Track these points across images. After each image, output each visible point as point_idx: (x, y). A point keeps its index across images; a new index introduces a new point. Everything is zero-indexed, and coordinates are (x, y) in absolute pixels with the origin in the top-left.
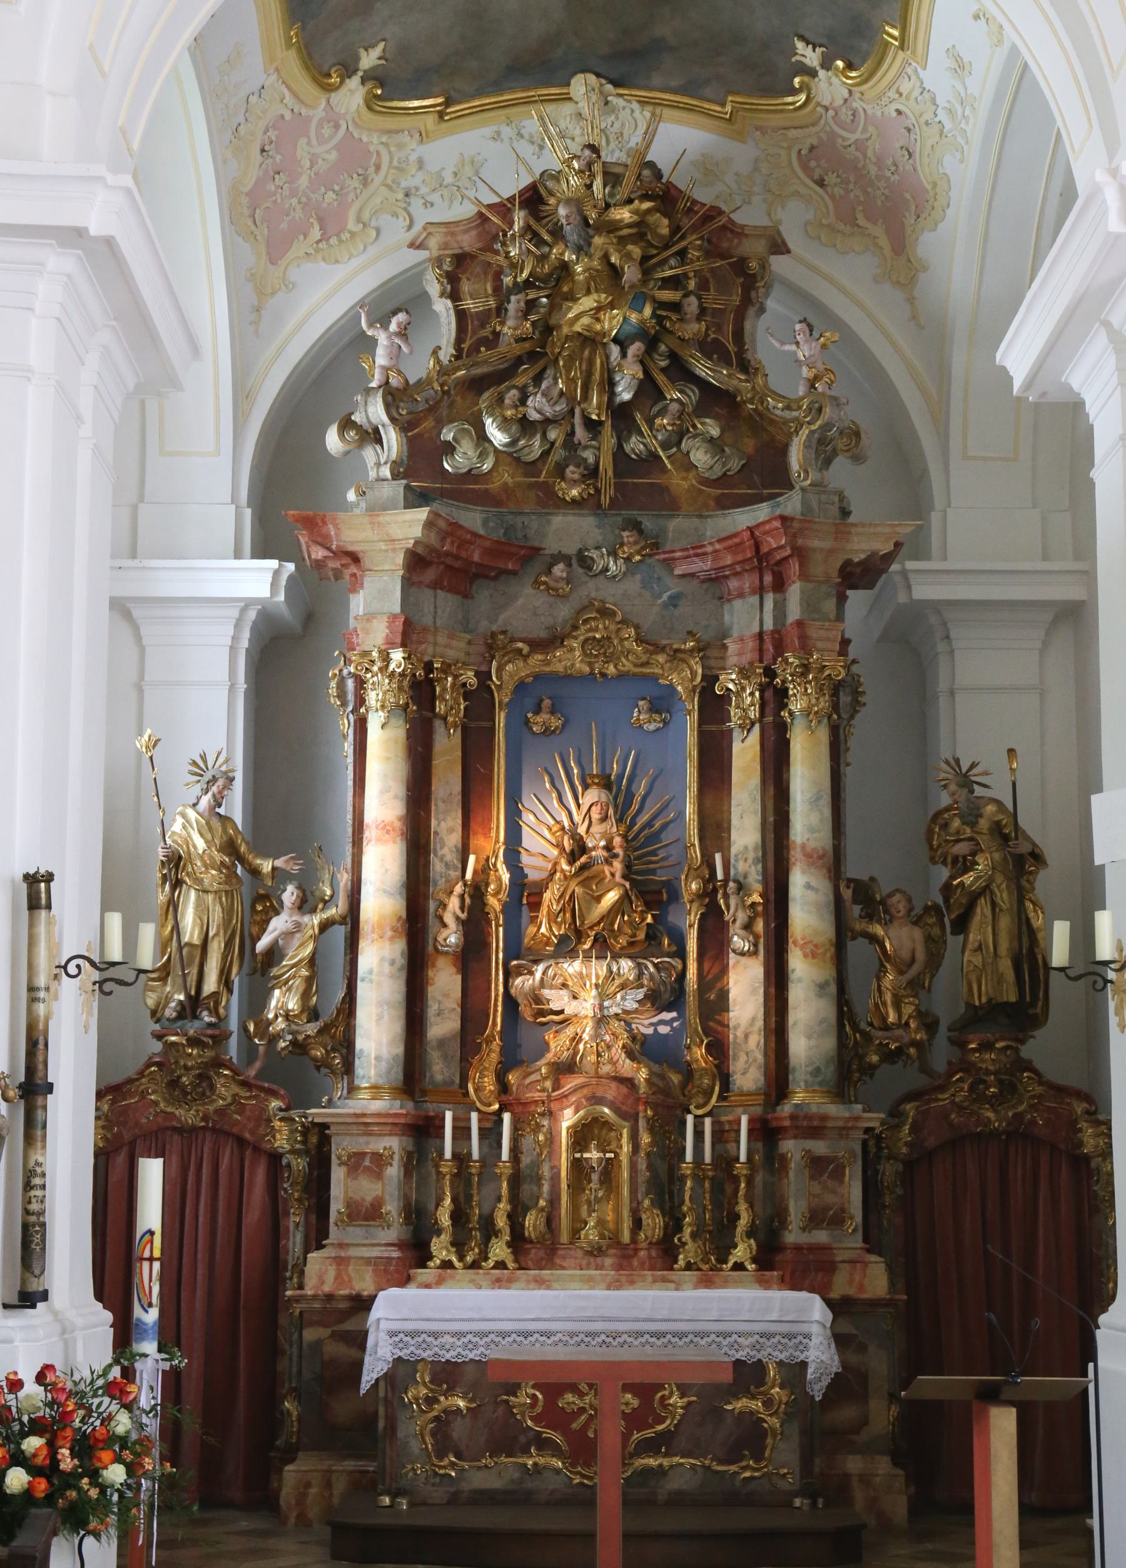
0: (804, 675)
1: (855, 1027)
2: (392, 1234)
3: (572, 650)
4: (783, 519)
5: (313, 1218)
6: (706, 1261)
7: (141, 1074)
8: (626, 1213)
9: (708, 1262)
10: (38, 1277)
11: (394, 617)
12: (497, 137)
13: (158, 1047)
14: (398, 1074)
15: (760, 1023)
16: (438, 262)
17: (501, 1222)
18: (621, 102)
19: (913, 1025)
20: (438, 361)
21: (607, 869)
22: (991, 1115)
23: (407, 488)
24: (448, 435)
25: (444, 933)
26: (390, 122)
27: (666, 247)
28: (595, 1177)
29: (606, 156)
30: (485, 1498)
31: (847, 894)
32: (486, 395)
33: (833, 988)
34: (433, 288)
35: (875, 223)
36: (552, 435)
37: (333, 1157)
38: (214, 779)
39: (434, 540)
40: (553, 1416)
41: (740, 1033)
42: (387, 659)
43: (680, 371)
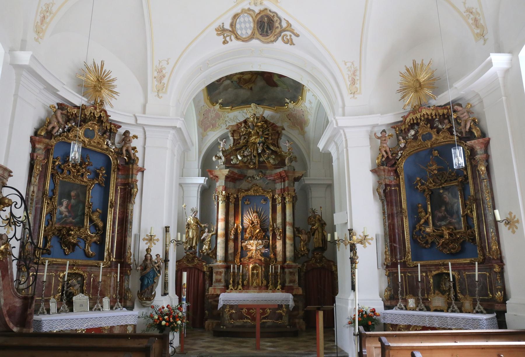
0: (288, 195)
1: (297, 251)
2: (223, 285)
3: (251, 191)
4: (285, 171)
5: (210, 282)
6: (273, 289)
7: (183, 259)
8: (260, 281)
9: (273, 289)
11: (223, 186)
12: (240, 113)
13: (185, 254)
14: (224, 259)
15: (282, 250)
16: (231, 131)
17: (240, 282)
18: (259, 107)
19: (306, 250)
20: (230, 146)
21: (257, 226)
22: (318, 265)
23: (226, 166)
24: (232, 158)
25: (231, 236)
26: (223, 110)
27: (266, 129)
28: (255, 275)
29: (257, 115)
30: (237, 327)
31: (295, 230)
32: (238, 152)
33: (293, 245)
34: (230, 135)
35: (298, 126)
36: (248, 158)
37: (213, 272)
38: (195, 212)
39: (230, 174)
40: (249, 313)
41: (278, 252)
42: (222, 193)
43: (268, 148)
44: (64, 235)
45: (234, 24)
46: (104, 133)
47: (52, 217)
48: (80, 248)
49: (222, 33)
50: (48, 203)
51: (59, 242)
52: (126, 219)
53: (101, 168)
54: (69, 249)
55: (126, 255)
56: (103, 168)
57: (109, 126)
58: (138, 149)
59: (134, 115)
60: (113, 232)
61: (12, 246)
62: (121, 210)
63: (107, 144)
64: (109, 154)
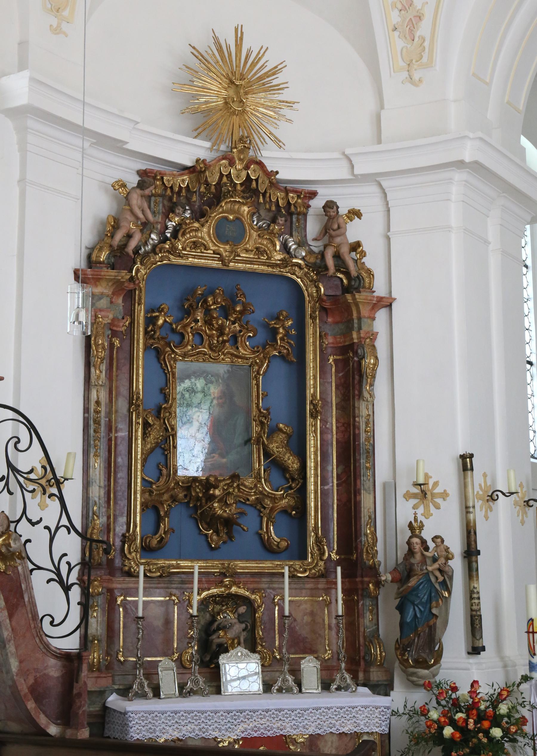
10: (479, 640)
44: (198, 499)
46: (274, 221)
47: (166, 456)
48: (244, 530)
50: (146, 425)
51: (191, 517)
52: (354, 441)
53: (280, 313)
54: (217, 532)
55: (361, 541)
56: (284, 313)
57: (283, 199)
58: (365, 247)
59: (344, 154)
60: (324, 482)
61: (23, 540)
62: (342, 421)
63: (285, 248)
64: (294, 274)
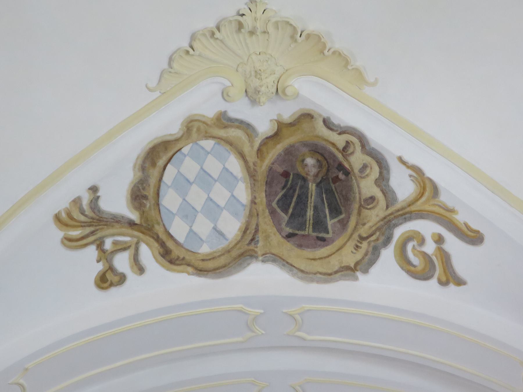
45: (150, 192)
49: (92, 233)
